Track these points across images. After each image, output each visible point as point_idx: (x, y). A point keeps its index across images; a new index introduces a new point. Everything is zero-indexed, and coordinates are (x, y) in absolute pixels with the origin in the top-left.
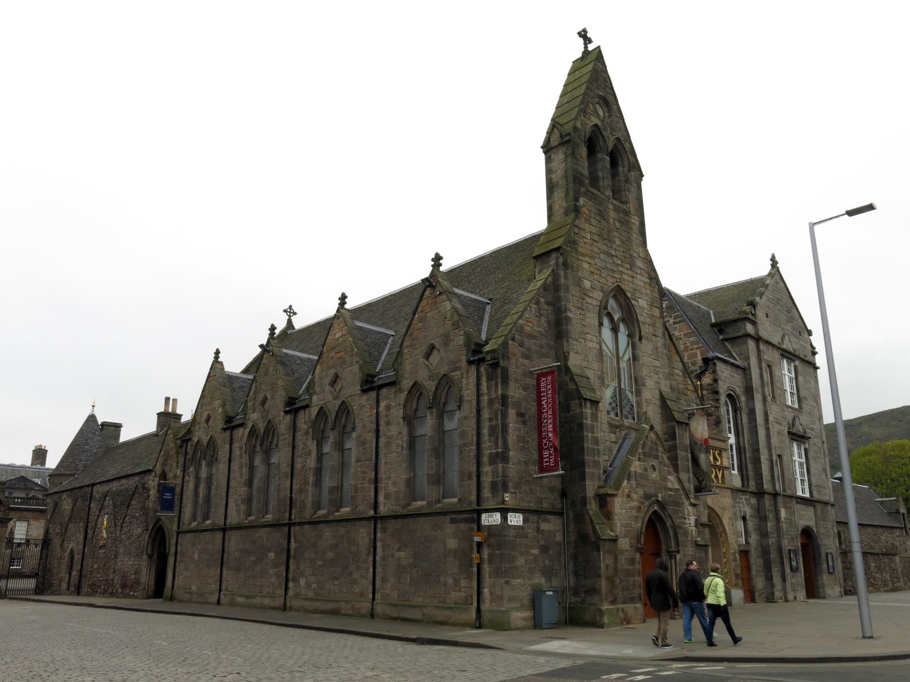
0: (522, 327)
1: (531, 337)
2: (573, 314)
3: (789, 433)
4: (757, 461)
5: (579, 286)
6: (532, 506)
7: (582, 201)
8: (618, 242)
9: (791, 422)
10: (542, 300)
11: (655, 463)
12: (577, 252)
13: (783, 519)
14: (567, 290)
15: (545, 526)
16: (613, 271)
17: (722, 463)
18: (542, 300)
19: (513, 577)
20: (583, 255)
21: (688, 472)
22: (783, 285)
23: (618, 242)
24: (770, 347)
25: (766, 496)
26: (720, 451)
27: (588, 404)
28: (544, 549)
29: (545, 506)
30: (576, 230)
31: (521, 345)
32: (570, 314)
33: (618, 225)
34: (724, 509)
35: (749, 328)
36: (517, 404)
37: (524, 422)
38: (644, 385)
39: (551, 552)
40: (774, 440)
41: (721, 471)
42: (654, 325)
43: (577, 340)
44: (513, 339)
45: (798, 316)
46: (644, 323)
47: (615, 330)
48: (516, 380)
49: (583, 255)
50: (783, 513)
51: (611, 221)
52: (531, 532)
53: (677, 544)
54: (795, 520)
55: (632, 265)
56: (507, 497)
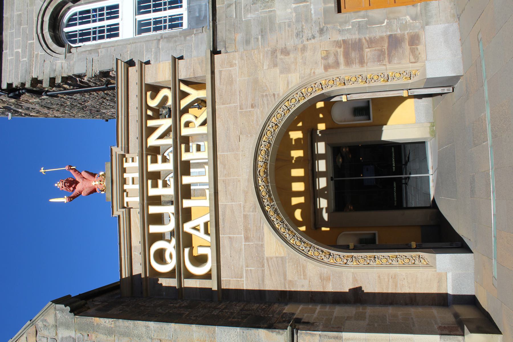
41: (184, 88)
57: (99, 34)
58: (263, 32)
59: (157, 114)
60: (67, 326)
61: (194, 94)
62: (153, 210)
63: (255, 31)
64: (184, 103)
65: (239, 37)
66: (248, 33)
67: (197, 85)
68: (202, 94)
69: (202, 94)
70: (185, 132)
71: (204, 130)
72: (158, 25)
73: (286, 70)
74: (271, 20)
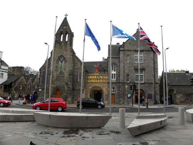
3: (134, 69)
4: (119, 76)
7: (56, 44)
8: (63, 48)
9: (136, 66)
11: (59, 82)
23: (63, 48)
24: (130, 51)
31: (43, 68)
33: (64, 45)
34: (104, 87)
35: (121, 49)
40: (126, 71)
42: (70, 59)
46: (67, 59)
47: (62, 62)
50: (126, 86)
51: (62, 45)
53: (62, 93)
72: (113, 76)
73: (105, 89)
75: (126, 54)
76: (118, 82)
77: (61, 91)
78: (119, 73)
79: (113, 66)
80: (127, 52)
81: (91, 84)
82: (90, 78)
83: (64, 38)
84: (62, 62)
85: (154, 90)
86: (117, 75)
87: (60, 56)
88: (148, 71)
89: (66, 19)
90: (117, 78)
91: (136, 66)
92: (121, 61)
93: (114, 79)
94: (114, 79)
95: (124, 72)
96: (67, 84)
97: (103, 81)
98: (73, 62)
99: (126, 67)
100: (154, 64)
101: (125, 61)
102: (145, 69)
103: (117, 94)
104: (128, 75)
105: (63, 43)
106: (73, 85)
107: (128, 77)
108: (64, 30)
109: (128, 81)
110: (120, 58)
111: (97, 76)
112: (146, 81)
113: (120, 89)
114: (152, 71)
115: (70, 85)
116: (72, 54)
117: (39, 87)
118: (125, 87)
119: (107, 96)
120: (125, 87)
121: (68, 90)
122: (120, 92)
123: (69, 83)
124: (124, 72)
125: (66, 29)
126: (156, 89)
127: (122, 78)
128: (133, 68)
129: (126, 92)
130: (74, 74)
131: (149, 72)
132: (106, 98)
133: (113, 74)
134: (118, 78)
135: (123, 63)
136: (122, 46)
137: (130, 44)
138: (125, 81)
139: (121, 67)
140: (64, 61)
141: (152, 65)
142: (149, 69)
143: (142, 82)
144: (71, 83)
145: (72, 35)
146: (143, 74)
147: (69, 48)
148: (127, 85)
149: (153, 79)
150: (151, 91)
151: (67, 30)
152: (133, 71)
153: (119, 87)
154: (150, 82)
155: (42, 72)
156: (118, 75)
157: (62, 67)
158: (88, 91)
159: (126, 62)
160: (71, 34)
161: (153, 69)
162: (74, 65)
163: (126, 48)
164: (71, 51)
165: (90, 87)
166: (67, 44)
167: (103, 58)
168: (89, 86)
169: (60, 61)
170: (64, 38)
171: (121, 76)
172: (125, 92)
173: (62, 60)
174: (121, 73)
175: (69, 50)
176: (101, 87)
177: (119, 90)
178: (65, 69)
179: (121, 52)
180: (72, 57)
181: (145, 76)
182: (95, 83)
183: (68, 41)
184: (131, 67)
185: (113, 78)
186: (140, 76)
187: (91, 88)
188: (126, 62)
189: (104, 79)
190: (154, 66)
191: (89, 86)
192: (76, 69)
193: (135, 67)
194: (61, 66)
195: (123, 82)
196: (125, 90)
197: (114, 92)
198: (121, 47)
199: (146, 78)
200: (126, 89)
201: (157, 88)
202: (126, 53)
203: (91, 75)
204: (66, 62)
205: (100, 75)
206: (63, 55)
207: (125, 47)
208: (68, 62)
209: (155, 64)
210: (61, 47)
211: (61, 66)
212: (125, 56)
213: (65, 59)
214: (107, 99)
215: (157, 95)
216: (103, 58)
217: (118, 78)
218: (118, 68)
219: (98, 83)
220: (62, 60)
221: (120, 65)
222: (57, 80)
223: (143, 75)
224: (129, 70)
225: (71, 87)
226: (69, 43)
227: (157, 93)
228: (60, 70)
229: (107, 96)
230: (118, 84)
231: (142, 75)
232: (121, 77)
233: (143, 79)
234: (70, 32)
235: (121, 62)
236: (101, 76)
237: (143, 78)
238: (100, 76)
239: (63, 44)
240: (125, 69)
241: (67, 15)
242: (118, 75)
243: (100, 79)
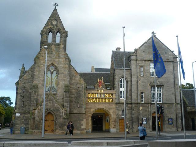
0: (23, 78)
1: (26, 79)
2: (36, 73)
4: (131, 95)
5: (39, 66)
6: (23, 112)
9: (152, 81)
10: (30, 71)
11: (51, 102)
12: (39, 59)
13: (140, 110)
14: (35, 68)
15: (26, 116)
16: (51, 60)
17: (112, 97)
18: (30, 71)
19: (16, 125)
20: (41, 59)
21: (68, 103)
22: (157, 40)
24: (144, 61)
25: (133, 104)
26: (112, 94)
27: (33, 92)
28: (25, 120)
29: (26, 112)
30: (40, 54)
32: (35, 73)
33: (55, 49)
36: (21, 93)
37: (22, 97)
38: (59, 84)
39: (27, 120)
43: (36, 78)
44: (20, 81)
45: (166, 47)
47: (52, 73)
48: (20, 89)
49: (41, 59)
50: (141, 108)
51: (53, 49)
52: (22, 117)
54: (149, 110)
55: (59, 57)
56: (16, 111)
57: (121, 85)
58: (118, 110)
59: (109, 96)
60: (85, 87)
61: (111, 100)
62: (97, 94)
63: (118, 109)
64: (110, 99)
65: (118, 106)
66: (118, 108)
67: (112, 101)
68: (111, 102)
69: (111, 102)
70: (106, 99)
71: (106, 102)
72: (121, 94)
73: (113, 112)
74: (119, 111)
75: (140, 65)
76: (129, 102)
77: (54, 116)
78: (131, 89)
79: (122, 79)
80: (140, 62)
81: (93, 105)
82: (92, 97)
83: (54, 37)
84: (52, 73)
85: (175, 112)
86: (127, 92)
87: (50, 65)
88: (168, 87)
89: (55, 10)
90: (127, 97)
91: (152, 81)
92: (132, 74)
93: (123, 98)
94: (123, 98)
95: (137, 89)
96: (63, 105)
97: (109, 101)
98: (69, 74)
99: (140, 82)
100: (174, 78)
101: (138, 74)
102: (163, 85)
103: (129, 118)
104: (142, 93)
105: (53, 45)
106: (70, 106)
107: (142, 96)
108: (54, 27)
109: (142, 101)
110: (131, 70)
111: (101, 94)
112: (165, 102)
113: (133, 112)
114: (172, 88)
115: (68, 107)
116: (67, 62)
117: (16, 111)
118: (140, 109)
119: (115, 121)
120: (138, 109)
121: (65, 114)
122: (133, 116)
123: (66, 104)
124: (137, 89)
125: (57, 25)
126: (177, 111)
127: (134, 96)
128: (149, 84)
129: (141, 116)
130: (71, 91)
131: (168, 89)
132: (113, 124)
133: (121, 92)
134: (129, 96)
135: (135, 76)
136: (134, 54)
137: (144, 52)
138: (139, 101)
139: (134, 83)
140: (55, 72)
141: (173, 80)
142: (169, 85)
143: (160, 102)
144: (68, 104)
145: (65, 35)
146: (161, 92)
147: (63, 53)
148: (142, 106)
149: (174, 98)
150: (172, 113)
151: (60, 27)
152: (149, 87)
153: (131, 109)
154: (170, 103)
155: (19, 87)
156: (129, 93)
157: (52, 81)
158: (89, 115)
159: (140, 75)
160: (65, 34)
161: (173, 86)
162: (71, 79)
163: (139, 58)
164: (66, 59)
165: (92, 110)
166: (59, 48)
167: (93, 67)
168: (90, 108)
169: (49, 72)
170: (54, 37)
171: (133, 94)
172: (140, 115)
173: (52, 71)
174: (133, 90)
175: (62, 56)
176: (107, 109)
177: (131, 113)
178: (58, 84)
179: (133, 62)
180: (67, 66)
181: (165, 95)
182: (98, 103)
183: (61, 43)
184: (146, 83)
185: (121, 97)
186: (158, 94)
187: (93, 111)
188: (140, 75)
189: (111, 98)
190: (174, 82)
191: (90, 108)
192: (73, 84)
193: (151, 82)
194: (51, 79)
195: (137, 102)
196: (140, 112)
197: (123, 115)
198: (133, 55)
199: (165, 97)
200: (141, 112)
201: (178, 110)
202: (139, 63)
203: (93, 92)
204: (58, 73)
205: (105, 92)
206: (54, 63)
207: (138, 55)
208: (62, 73)
209: (176, 79)
210: (51, 51)
211: (51, 79)
212: (138, 67)
213: (56, 69)
214: (115, 125)
215: (179, 119)
216: (93, 67)
217: (129, 96)
218: (129, 84)
219: (103, 103)
220: (52, 71)
221: (132, 80)
222: (48, 99)
223: (161, 93)
224: (143, 86)
225: (68, 109)
226: (62, 46)
227: (179, 117)
228: (50, 85)
229: (115, 121)
230: (129, 105)
231: (159, 93)
232: (133, 96)
233: (161, 98)
234: (63, 31)
235: (134, 75)
236: (106, 94)
237: (161, 97)
238: (105, 94)
239: (53, 47)
240: (138, 84)
241: (57, 5)
242: (129, 93)
243: (105, 98)
